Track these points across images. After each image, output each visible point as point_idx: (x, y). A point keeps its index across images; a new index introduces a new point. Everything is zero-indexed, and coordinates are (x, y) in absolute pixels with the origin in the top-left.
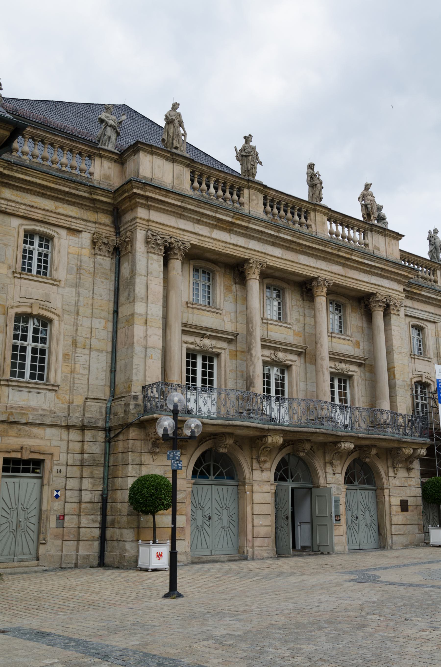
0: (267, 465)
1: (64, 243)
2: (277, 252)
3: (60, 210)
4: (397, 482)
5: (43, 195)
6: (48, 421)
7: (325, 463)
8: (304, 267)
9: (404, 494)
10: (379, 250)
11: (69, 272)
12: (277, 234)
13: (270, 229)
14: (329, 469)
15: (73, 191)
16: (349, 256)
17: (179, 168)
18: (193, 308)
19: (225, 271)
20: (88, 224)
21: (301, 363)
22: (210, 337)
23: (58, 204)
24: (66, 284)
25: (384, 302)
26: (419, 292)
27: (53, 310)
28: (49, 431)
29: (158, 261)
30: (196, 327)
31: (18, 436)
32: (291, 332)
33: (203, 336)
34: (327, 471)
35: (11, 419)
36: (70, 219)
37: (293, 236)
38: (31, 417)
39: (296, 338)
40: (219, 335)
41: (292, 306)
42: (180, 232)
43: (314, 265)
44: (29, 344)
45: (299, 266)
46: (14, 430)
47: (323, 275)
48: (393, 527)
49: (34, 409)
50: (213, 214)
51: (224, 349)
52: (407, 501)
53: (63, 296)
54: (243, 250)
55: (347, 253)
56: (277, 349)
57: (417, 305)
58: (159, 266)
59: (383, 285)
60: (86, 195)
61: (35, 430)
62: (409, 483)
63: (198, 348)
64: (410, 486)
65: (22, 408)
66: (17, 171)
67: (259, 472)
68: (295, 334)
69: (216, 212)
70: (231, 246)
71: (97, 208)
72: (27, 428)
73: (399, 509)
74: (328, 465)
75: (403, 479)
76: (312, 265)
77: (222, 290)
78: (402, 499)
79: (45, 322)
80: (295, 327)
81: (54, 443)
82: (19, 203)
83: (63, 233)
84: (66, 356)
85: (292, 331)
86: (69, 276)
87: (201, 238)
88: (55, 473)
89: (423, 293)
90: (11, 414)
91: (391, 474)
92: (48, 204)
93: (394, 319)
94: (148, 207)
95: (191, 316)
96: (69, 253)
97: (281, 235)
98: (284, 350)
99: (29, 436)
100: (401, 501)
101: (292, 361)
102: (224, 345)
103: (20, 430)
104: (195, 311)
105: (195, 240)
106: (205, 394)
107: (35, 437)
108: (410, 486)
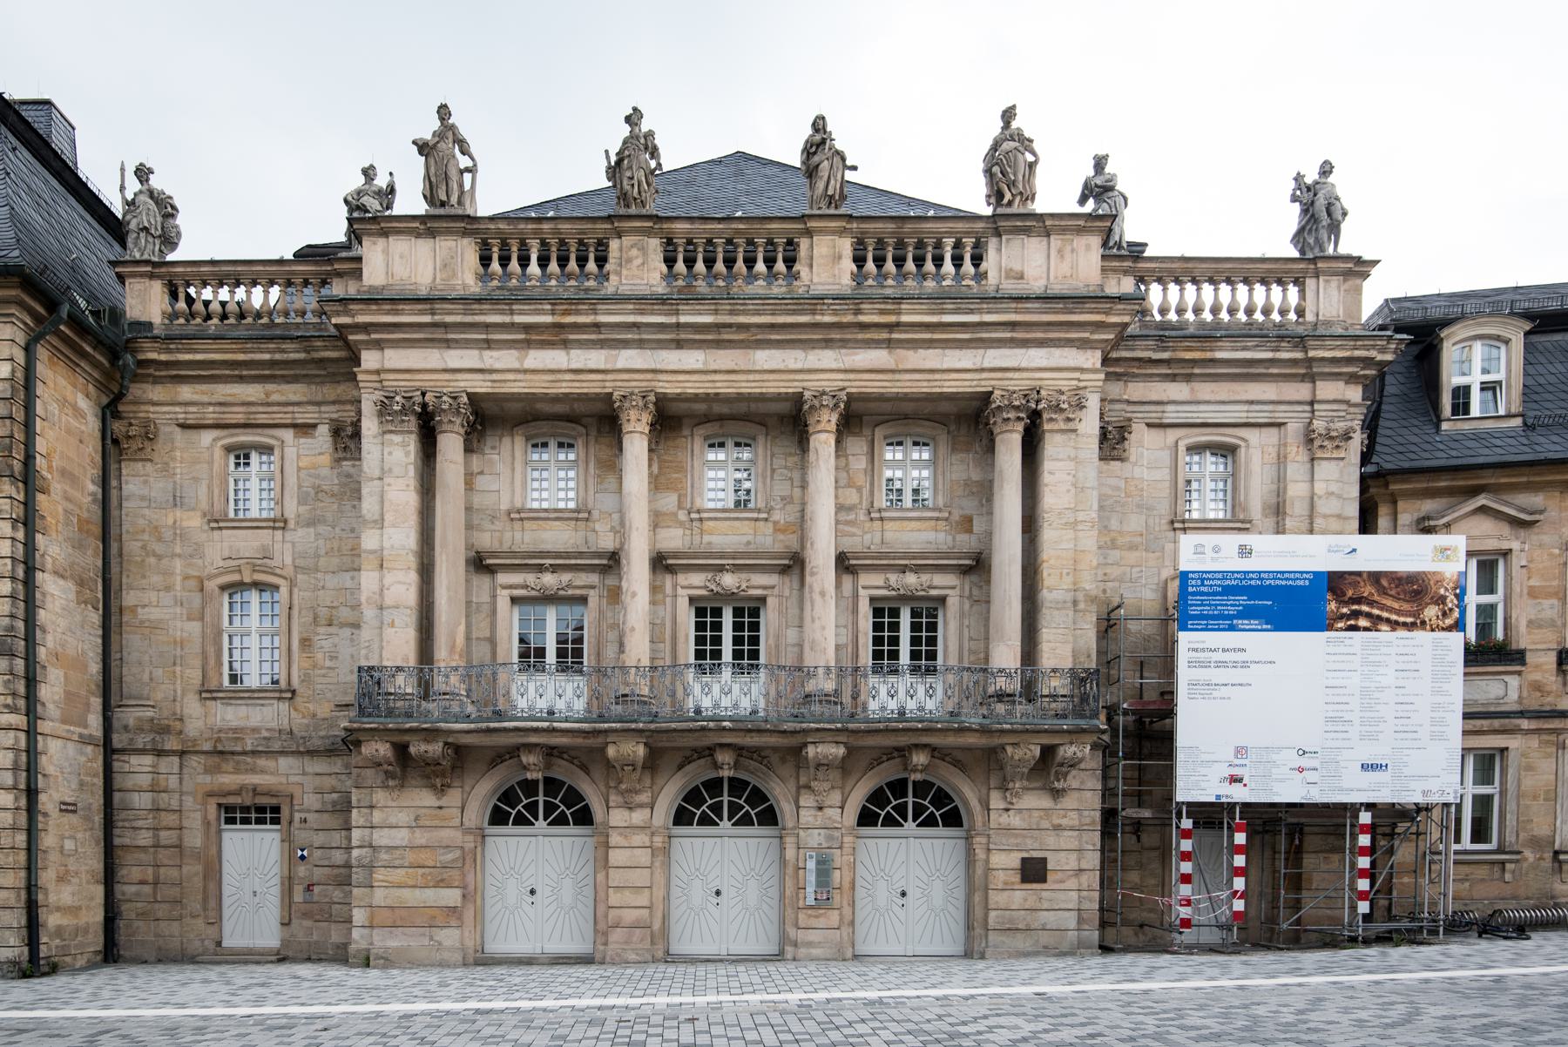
0: (644, 798)
3: (275, 398)
4: (1015, 820)
5: (241, 379)
7: (799, 788)
9: (1036, 846)
14: (807, 800)
18: (521, 519)
19: (599, 431)
21: (791, 589)
22: (555, 569)
23: (270, 387)
26: (1209, 355)
30: (513, 554)
32: (768, 528)
33: (540, 569)
34: (802, 803)
36: (290, 409)
39: (781, 537)
40: (573, 562)
41: (773, 471)
48: (992, 914)
51: (593, 587)
52: (1044, 860)
62: (1056, 821)
63: (534, 593)
64: (1058, 828)
67: (626, 813)
68: (778, 529)
71: (334, 374)
73: (1018, 878)
74: (803, 791)
75: (1036, 814)
77: (592, 470)
78: (1026, 855)
80: (777, 516)
82: (203, 404)
85: (770, 525)
89: (1219, 355)
91: (996, 801)
92: (252, 392)
93: (1054, 448)
95: (518, 535)
98: (737, 568)
100: (1023, 860)
101: (765, 588)
102: (594, 578)
104: (527, 524)
106: (561, 677)
108: (1058, 828)
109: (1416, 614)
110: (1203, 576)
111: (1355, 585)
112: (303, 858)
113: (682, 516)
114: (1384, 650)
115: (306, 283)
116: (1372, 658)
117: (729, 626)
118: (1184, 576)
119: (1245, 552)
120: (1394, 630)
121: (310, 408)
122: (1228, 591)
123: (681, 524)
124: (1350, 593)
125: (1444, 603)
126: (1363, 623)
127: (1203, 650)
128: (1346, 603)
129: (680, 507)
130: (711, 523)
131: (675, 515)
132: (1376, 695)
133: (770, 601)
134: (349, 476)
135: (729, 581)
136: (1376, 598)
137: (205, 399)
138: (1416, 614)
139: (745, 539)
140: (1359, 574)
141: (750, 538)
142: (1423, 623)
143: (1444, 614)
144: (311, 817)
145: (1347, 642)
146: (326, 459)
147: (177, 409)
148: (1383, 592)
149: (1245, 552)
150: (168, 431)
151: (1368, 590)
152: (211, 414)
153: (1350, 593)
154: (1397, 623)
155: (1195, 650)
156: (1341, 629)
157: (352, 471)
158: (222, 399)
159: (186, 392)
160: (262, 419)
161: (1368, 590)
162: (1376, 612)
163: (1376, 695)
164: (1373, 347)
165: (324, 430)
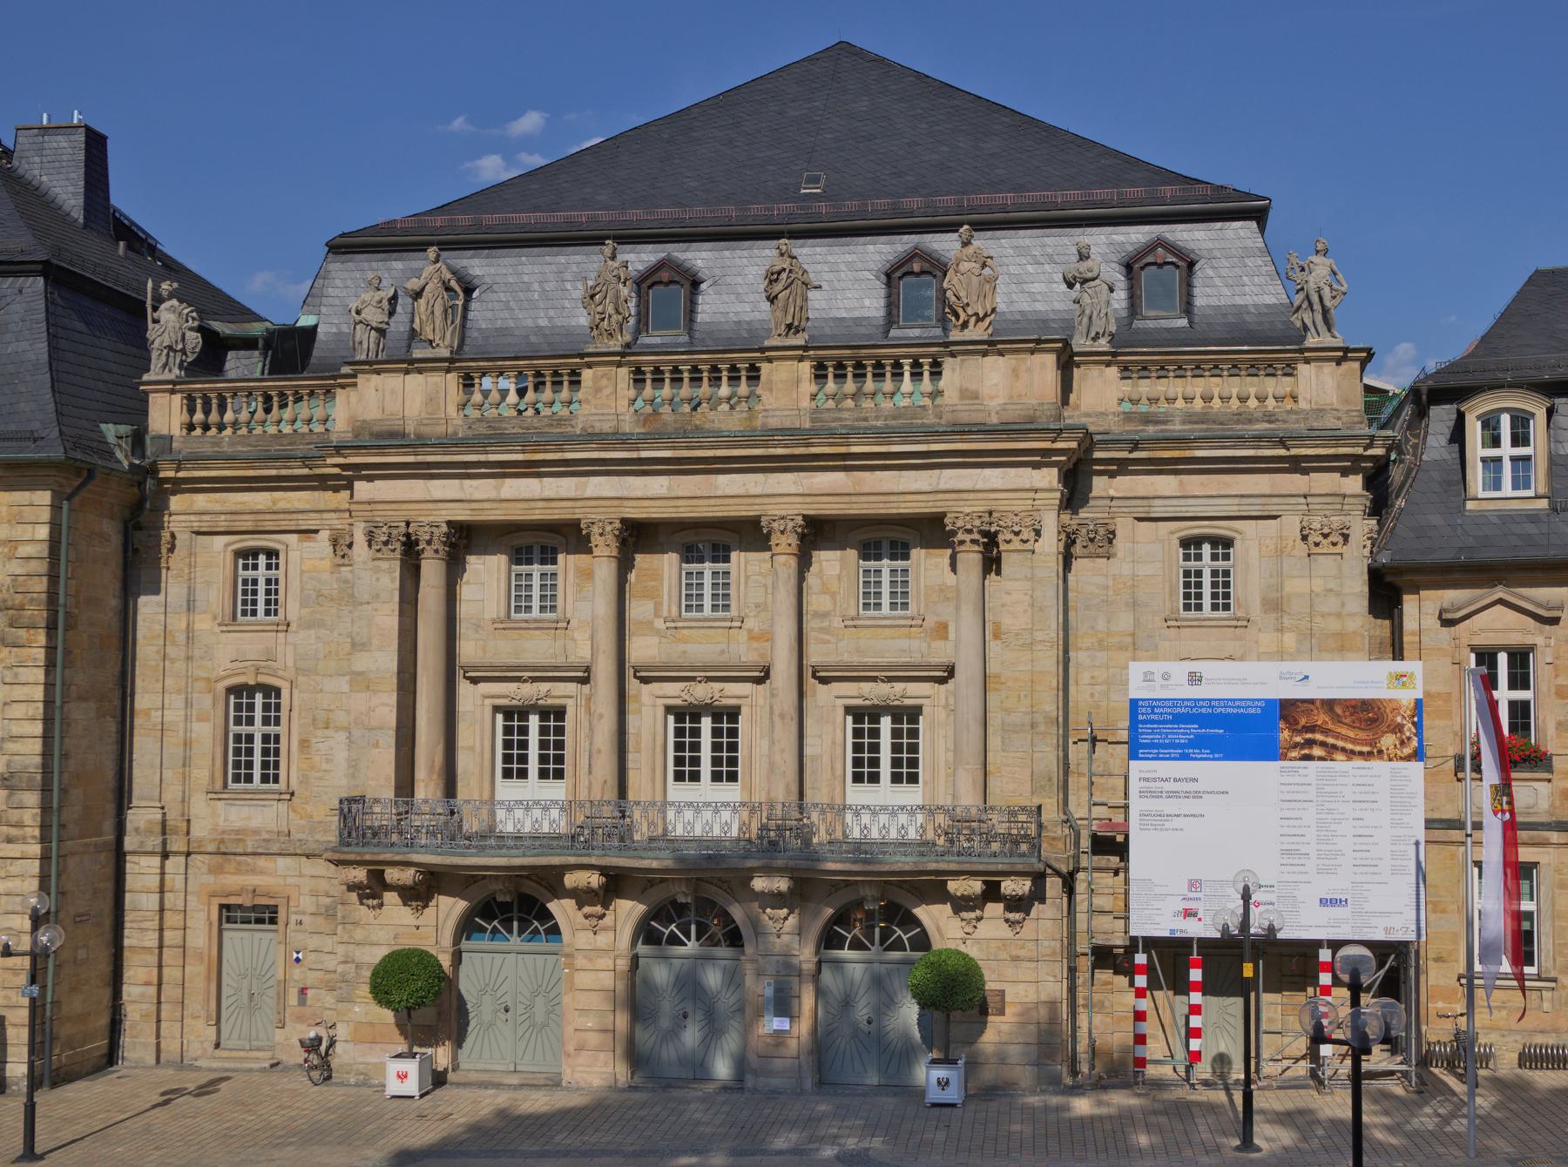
1: (294, 556)
2: (658, 485)
3: (282, 505)
6: (275, 848)
8: (727, 501)
10: (977, 398)
11: (304, 603)
12: (634, 455)
13: (615, 450)
15: (284, 472)
16: (843, 450)
17: (435, 379)
20: (325, 515)
24: (300, 625)
25: (969, 531)
26: (1188, 454)
27: (281, 673)
28: (281, 861)
29: (390, 571)
30: (493, 668)
31: (238, 872)
32: (742, 636)
35: (223, 849)
36: (295, 516)
37: (674, 448)
38: (250, 844)
39: (755, 645)
41: (747, 577)
42: (430, 506)
43: (758, 491)
44: (258, 730)
45: (712, 502)
46: (231, 866)
47: (773, 509)
49: (256, 832)
50: (482, 458)
53: (295, 646)
54: (569, 504)
55: (831, 445)
56: (693, 679)
57: (1195, 484)
58: (393, 581)
59: (979, 486)
60: (305, 471)
61: (262, 862)
63: (515, 702)
65: (237, 832)
66: (194, 469)
69: (487, 453)
70: (540, 504)
72: (249, 859)
76: (753, 491)
79: (271, 691)
80: (750, 623)
81: (290, 881)
83: (292, 539)
84: (305, 744)
86: (305, 611)
87: (474, 506)
88: (292, 925)
90: (222, 841)
94: (370, 479)
96: (302, 572)
97: (644, 454)
99: (254, 871)
102: (571, 687)
103: (240, 863)
105: (462, 514)
107: (262, 873)
109: (1372, 744)
110: (1153, 704)
111: (1308, 713)
112: (298, 960)
113: (659, 624)
114: (1340, 780)
115: (311, 394)
116: (1328, 789)
117: (706, 735)
118: (1134, 703)
119: (1195, 679)
120: (1349, 759)
121: (313, 515)
122: (1179, 719)
123: (658, 632)
124: (1303, 721)
125: (1401, 732)
126: (1317, 751)
127: (1154, 780)
128: (1299, 732)
129: (657, 615)
130: (685, 632)
131: (651, 623)
132: (1333, 827)
133: (744, 710)
134: (346, 581)
135: (701, 692)
136: (1330, 726)
137: (218, 508)
138: (1372, 744)
139: (719, 648)
140: (1312, 701)
141: (724, 646)
142: (1380, 752)
143: (1402, 743)
144: (306, 919)
145: (1302, 772)
146: (326, 564)
147: (192, 518)
148: (1338, 720)
149: (1195, 679)
150: (182, 539)
151: (1321, 718)
152: (223, 523)
153: (1303, 721)
154: (1353, 752)
155: (1146, 780)
156: (1295, 759)
157: (350, 576)
158: (233, 508)
159: (201, 501)
160: (269, 526)
161: (1321, 718)
162: (1331, 741)
163: (1333, 827)
164: (1358, 445)
165: (324, 535)
